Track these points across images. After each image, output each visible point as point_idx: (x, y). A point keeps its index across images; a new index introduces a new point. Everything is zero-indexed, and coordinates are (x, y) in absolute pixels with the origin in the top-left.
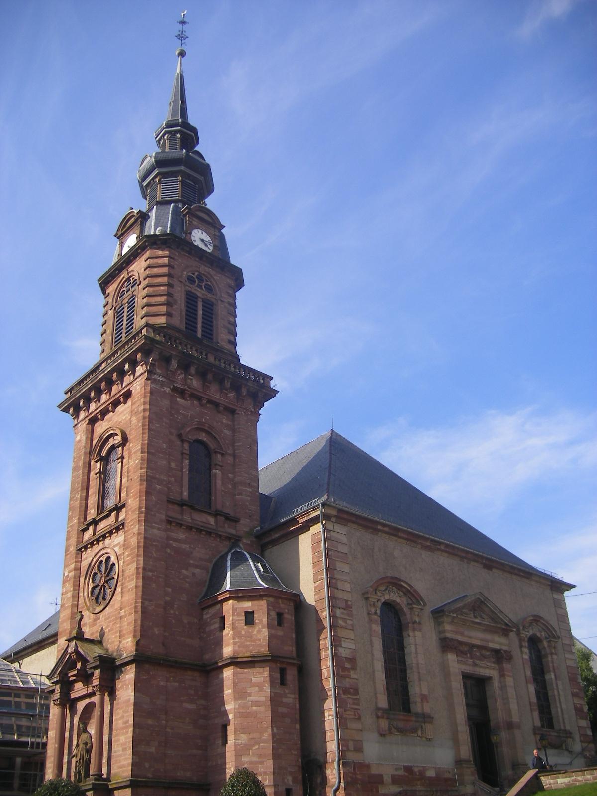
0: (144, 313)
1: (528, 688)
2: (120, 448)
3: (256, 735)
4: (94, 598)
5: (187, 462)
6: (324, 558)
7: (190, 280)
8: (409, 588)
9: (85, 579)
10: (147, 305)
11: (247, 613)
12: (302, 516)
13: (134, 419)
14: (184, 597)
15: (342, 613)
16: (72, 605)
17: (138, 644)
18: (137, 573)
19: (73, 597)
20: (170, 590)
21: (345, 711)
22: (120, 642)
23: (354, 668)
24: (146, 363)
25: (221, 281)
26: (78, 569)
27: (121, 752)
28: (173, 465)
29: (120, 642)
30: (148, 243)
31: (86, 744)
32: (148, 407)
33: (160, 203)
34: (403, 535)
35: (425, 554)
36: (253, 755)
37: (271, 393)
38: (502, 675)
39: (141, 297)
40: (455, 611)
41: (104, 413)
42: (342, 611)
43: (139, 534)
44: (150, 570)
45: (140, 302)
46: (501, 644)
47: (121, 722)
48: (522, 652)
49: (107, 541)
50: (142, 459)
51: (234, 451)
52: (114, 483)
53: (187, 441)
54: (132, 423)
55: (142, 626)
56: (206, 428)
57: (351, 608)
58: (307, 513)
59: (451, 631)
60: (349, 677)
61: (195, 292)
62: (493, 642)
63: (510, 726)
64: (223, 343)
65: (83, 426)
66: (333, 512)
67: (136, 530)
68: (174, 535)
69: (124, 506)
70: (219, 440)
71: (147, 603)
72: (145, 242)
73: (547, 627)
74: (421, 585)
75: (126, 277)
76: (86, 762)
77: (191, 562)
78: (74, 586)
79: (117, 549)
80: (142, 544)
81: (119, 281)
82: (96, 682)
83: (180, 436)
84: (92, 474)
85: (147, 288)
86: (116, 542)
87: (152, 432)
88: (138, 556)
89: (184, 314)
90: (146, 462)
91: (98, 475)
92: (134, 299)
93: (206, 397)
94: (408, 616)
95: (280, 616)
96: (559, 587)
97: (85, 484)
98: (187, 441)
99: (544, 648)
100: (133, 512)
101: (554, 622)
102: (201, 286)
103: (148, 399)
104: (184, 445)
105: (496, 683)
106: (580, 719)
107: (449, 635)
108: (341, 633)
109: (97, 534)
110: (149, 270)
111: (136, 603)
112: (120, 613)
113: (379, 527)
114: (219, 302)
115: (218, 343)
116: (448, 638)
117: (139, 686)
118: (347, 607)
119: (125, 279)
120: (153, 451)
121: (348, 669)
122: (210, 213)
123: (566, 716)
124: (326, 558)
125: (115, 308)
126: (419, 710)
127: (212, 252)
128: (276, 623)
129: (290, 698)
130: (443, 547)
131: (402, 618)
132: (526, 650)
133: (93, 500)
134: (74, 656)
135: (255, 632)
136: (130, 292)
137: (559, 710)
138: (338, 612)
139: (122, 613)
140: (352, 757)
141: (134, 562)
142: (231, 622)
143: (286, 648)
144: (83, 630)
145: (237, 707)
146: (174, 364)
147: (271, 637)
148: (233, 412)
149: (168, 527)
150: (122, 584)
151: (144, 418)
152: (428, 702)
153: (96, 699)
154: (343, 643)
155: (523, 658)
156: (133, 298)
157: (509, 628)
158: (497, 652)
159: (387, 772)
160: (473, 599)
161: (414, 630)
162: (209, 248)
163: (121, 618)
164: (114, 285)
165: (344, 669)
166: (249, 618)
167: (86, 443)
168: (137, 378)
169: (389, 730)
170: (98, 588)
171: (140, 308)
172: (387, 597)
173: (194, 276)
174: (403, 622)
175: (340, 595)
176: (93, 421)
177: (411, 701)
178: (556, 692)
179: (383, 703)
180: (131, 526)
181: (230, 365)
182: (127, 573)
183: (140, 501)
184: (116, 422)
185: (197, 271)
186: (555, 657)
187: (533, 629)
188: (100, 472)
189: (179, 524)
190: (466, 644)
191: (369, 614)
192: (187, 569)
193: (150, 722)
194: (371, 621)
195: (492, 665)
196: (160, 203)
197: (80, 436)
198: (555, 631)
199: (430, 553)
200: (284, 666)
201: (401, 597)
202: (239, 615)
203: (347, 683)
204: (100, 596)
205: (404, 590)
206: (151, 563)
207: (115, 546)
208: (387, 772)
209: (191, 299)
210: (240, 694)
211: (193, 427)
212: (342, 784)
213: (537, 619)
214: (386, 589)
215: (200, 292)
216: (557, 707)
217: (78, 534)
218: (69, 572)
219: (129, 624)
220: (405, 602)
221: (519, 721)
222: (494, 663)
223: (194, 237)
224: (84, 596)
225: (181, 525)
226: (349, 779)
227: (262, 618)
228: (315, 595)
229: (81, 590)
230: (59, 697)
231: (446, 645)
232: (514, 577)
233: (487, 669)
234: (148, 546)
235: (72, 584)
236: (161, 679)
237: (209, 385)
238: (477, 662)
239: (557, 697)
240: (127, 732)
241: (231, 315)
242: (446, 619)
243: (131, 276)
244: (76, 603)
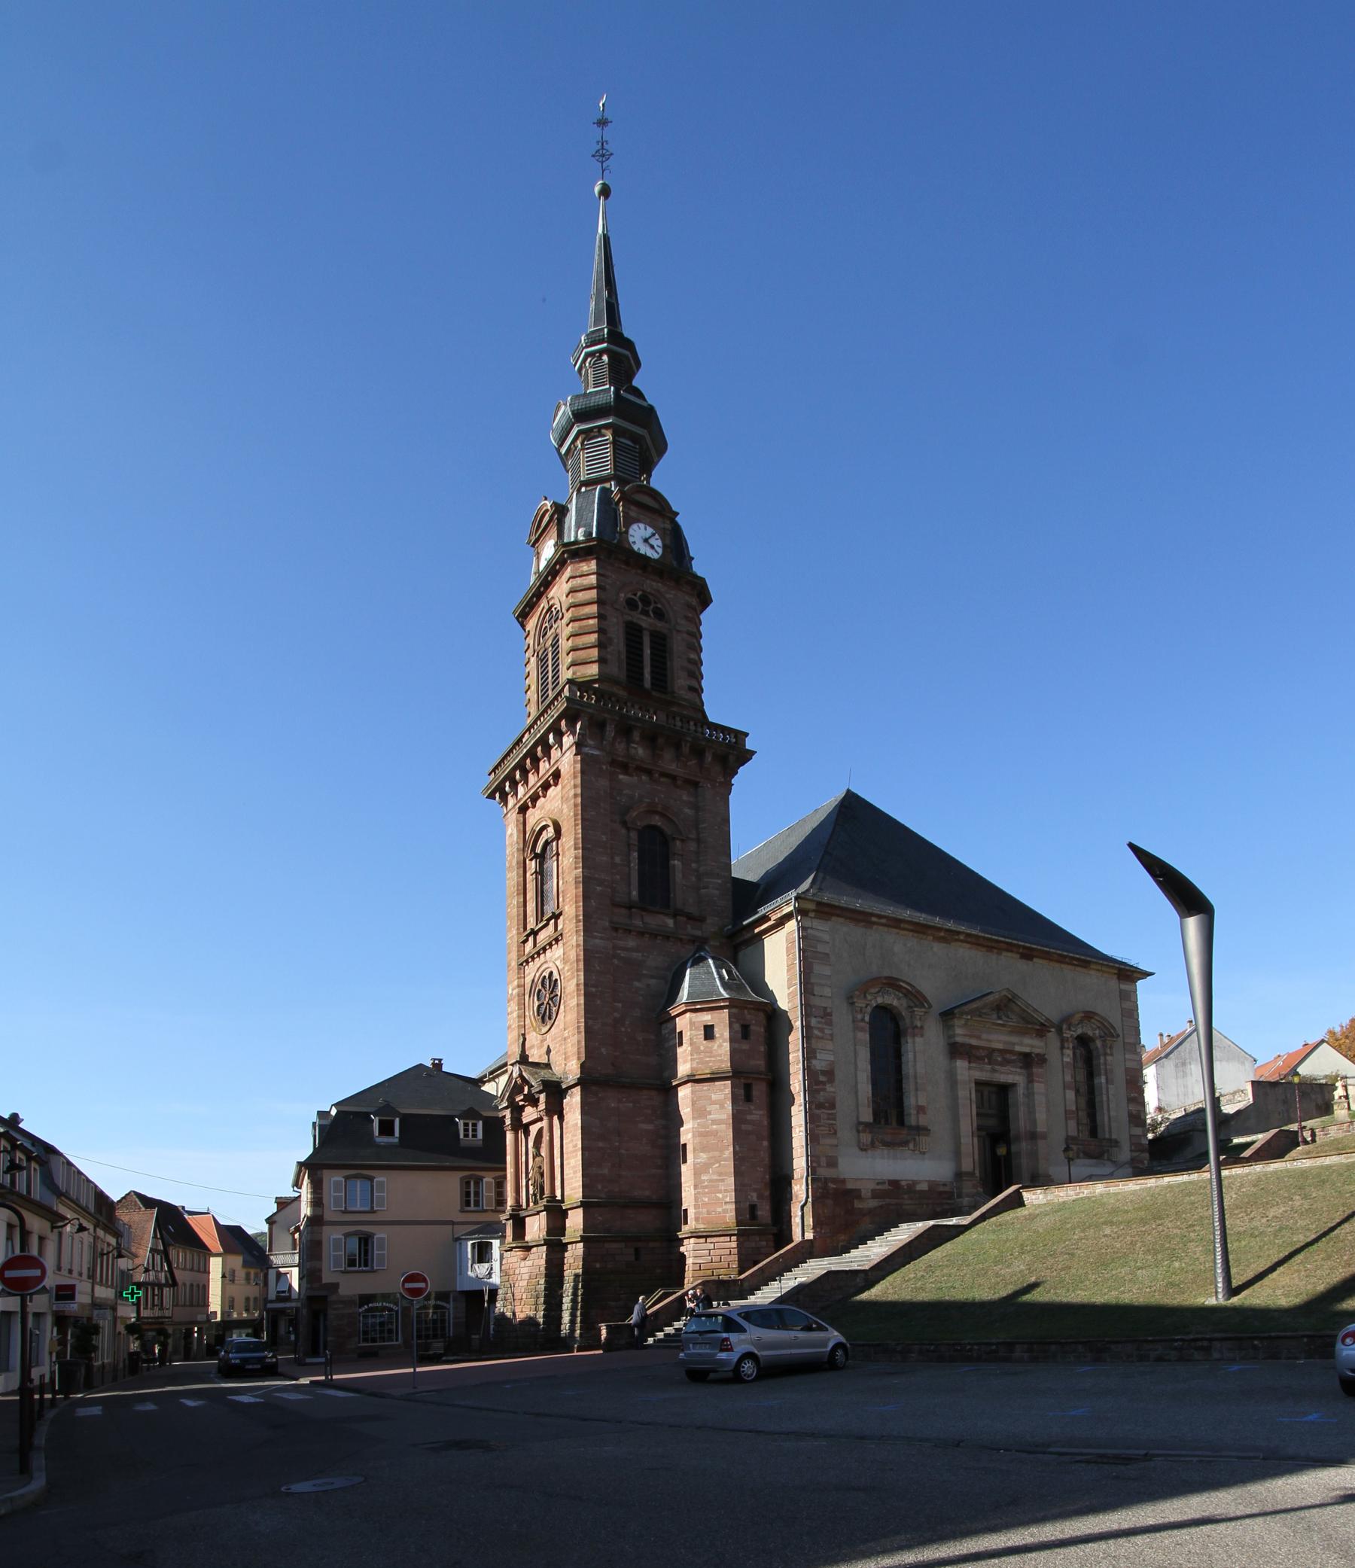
0: (569, 660)
3: (717, 1154)
5: (635, 854)
6: (797, 961)
10: (574, 649)
12: (773, 911)
13: (565, 806)
15: (819, 1022)
17: (582, 1066)
20: (620, 1005)
21: (818, 1126)
22: (566, 1065)
24: (573, 733)
25: (674, 598)
28: (617, 860)
29: (566, 1065)
32: (579, 791)
36: (713, 1173)
42: (820, 1020)
43: (578, 946)
50: (576, 858)
57: (831, 1016)
58: (779, 907)
66: (811, 906)
68: (621, 943)
69: (561, 914)
70: (677, 822)
72: (563, 553)
80: (582, 957)
83: (624, 823)
87: (587, 823)
88: (578, 970)
89: (623, 656)
90: (581, 860)
103: (579, 781)
108: (814, 1044)
111: (578, 1022)
112: (563, 1035)
115: (674, 692)
118: (826, 1015)
120: (589, 846)
121: (824, 1084)
122: (655, 495)
127: (661, 557)
128: (740, 1035)
129: (758, 1115)
135: (715, 1048)
138: (814, 1021)
140: (824, 1172)
142: (688, 1038)
143: (753, 1062)
145: (696, 1126)
146: (610, 731)
147: (733, 1052)
149: (615, 934)
151: (575, 805)
154: (818, 1055)
162: (656, 552)
163: (565, 1039)
168: (565, 752)
175: (816, 1001)
183: (577, 907)
185: (641, 590)
191: (854, 1021)
193: (601, 1144)
200: (749, 1081)
202: (697, 1029)
203: (821, 1097)
209: (633, 633)
210: (699, 1113)
212: (810, 1200)
215: (646, 622)
223: (633, 536)
225: (630, 931)
226: (818, 1194)
227: (723, 1032)
234: (591, 959)
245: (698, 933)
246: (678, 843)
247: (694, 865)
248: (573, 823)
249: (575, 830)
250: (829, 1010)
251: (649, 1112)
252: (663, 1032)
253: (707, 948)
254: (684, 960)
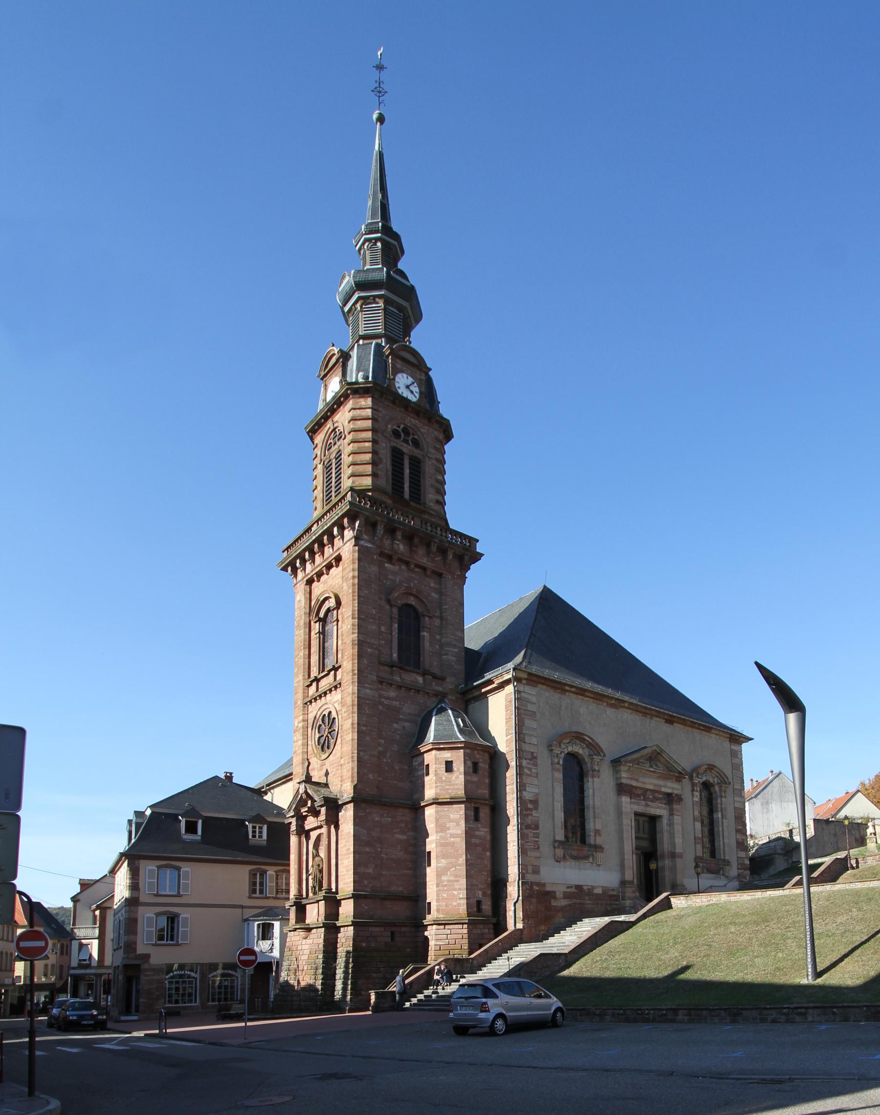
0: (350, 472)
1: (694, 825)
2: (335, 612)
3: (453, 860)
4: (320, 747)
5: (396, 625)
6: (514, 716)
7: (396, 434)
8: (591, 741)
9: (312, 729)
10: (354, 464)
11: (447, 762)
12: (497, 677)
13: (345, 584)
14: (395, 748)
15: (528, 763)
16: (303, 752)
17: (355, 787)
18: (353, 728)
19: (303, 745)
20: (382, 741)
21: (527, 842)
22: (341, 785)
23: (536, 808)
24: (353, 529)
25: (427, 432)
26: (306, 720)
27: (345, 873)
28: (383, 629)
29: (341, 785)
30: (352, 390)
31: (319, 865)
32: (356, 574)
33: (364, 337)
34: (589, 695)
35: (610, 711)
36: (451, 875)
37: (476, 557)
38: (671, 814)
39: (347, 455)
40: (631, 761)
41: (319, 575)
42: (528, 761)
43: (353, 693)
44: (364, 725)
45: (346, 460)
46: (673, 789)
47: (344, 849)
48: (693, 795)
50: (353, 625)
51: (441, 613)
52: (332, 643)
53: (395, 606)
54: (344, 588)
55: (358, 773)
56: (414, 593)
57: (537, 759)
59: (627, 778)
60: (531, 815)
61: (401, 448)
62: (666, 786)
63: (673, 855)
64: (431, 504)
65: (301, 587)
67: (350, 690)
68: (385, 693)
69: (340, 667)
70: (426, 603)
71: (362, 753)
73: (721, 776)
74: (602, 741)
75: (332, 428)
76: (319, 880)
77: (401, 717)
78: (303, 735)
79: (336, 705)
80: (356, 703)
81: (325, 432)
82: (322, 817)
83: (389, 601)
84: (313, 633)
85: (351, 445)
86: (335, 699)
87: (362, 599)
88: (353, 713)
89: (390, 473)
90: (357, 627)
91: (318, 635)
92: (341, 455)
93: (414, 562)
94: (589, 765)
95: (475, 765)
96: (737, 738)
97: (307, 643)
98: (395, 606)
99: (716, 792)
100: (347, 674)
101: (728, 771)
102: (408, 441)
103: (356, 566)
104: (393, 610)
105: (665, 821)
106: (741, 851)
107: (624, 781)
108: (527, 780)
109: (319, 690)
110: (353, 424)
111: (352, 753)
112: (340, 761)
113: (567, 688)
114: (427, 458)
115: (426, 503)
116: (623, 783)
117: (358, 821)
118: (533, 758)
119: (330, 430)
120: (363, 617)
121: (531, 810)
122: (415, 353)
123: (726, 849)
124: (516, 716)
125: (324, 462)
126: (592, 842)
127: (419, 400)
128: (471, 770)
129: (483, 832)
130: (626, 705)
131: (583, 767)
132: (697, 794)
133: (315, 658)
134: (304, 796)
135: (453, 778)
136: (336, 446)
137: (721, 843)
138: (524, 762)
139: (342, 761)
140: (530, 878)
141: (349, 718)
142: (434, 770)
143: (480, 791)
144: (311, 775)
145: (438, 838)
146: (380, 530)
147: (467, 782)
148: (440, 575)
149: (380, 686)
150: (341, 737)
151: (354, 585)
152: (600, 835)
153: (324, 830)
154: (527, 788)
155: (693, 801)
156: (338, 457)
157: (681, 775)
158: (669, 795)
159: (560, 891)
160: (650, 751)
161: (593, 777)
162: (415, 396)
163: (341, 765)
164: (321, 435)
165: (528, 809)
166: (449, 767)
167: (305, 604)
168: (346, 543)
169: (564, 857)
170: (323, 738)
171: (347, 467)
172: (570, 749)
173: (400, 430)
174: (584, 770)
175: (526, 747)
176: (310, 582)
177: (586, 835)
178: (721, 829)
179: (560, 836)
181: (436, 528)
182: (345, 727)
183: (353, 664)
184: (331, 585)
185: (402, 423)
186: (724, 799)
187: (706, 776)
188: (319, 632)
189: (389, 683)
190: (640, 788)
191: (552, 764)
192: (397, 723)
194: (553, 769)
195: (664, 806)
196: (364, 337)
197: (300, 597)
198: (728, 778)
199: (614, 710)
200: (478, 806)
201: (583, 749)
202: (440, 763)
203: (529, 820)
204: (325, 745)
205: (587, 743)
207: (334, 702)
208: (560, 891)
209: (397, 456)
210: (441, 828)
211: (401, 592)
212: (520, 898)
213: (711, 767)
214: (569, 743)
215: (406, 449)
216: (720, 841)
217: (304, 689)
218: (298, 723)
219: (347, 771)
220: (587, 753)
221: (681, 851)
222: (665, 804)
223: (398, 383)
224: (312, 745)
225: (391, 685)
226: (527, 894)
227: (459, 767)
228: (506, 747)
229: (309, 739)
230: (295, 829)
231: (622, 789)
232: (695, 730)
233: (658, 809)
234: (363, 704)
235: (301, 734)
236: (376, 815)
237: (416, 549)
238: (650, 803)
239: (721, 833)
240: (349, 857)
241: (439, 473)
242: (623, 768)
243: (336, 428)
244: (306, 750)
245: (441, 689)
246: (427, 619)
247: (438, 637)
248: (351, 598)
249: (353, 603)
250: (535, 755)
251: (403, 825)
252: (414, 764)
253: (446, 701)
254: (430, 709)
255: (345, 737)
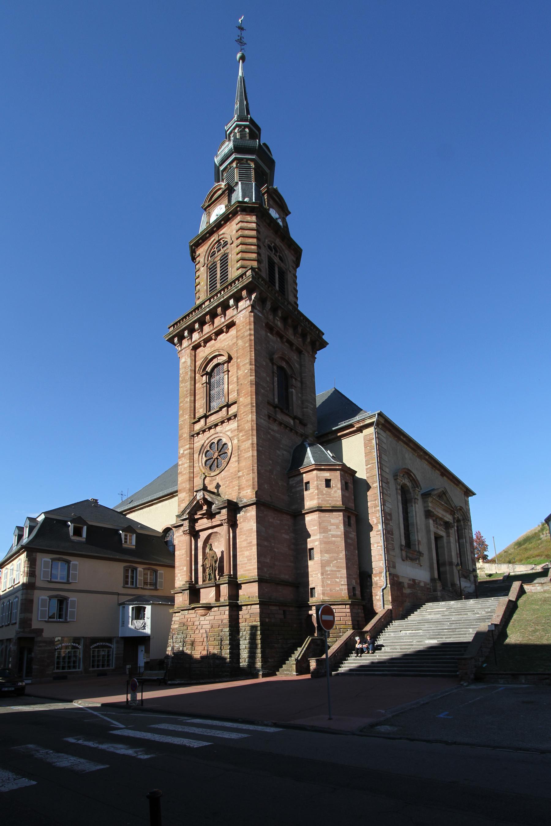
5: (276, 379)
49: (218, 429)
95: (346, 483)
135: (332, 492)
154: (386, 504)
166: (328, 483)
180: (244, 416)
202: (321, 481)
206: (261, 442)
255: (243, 455)
